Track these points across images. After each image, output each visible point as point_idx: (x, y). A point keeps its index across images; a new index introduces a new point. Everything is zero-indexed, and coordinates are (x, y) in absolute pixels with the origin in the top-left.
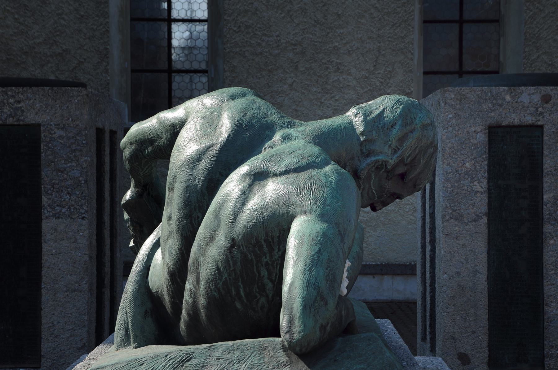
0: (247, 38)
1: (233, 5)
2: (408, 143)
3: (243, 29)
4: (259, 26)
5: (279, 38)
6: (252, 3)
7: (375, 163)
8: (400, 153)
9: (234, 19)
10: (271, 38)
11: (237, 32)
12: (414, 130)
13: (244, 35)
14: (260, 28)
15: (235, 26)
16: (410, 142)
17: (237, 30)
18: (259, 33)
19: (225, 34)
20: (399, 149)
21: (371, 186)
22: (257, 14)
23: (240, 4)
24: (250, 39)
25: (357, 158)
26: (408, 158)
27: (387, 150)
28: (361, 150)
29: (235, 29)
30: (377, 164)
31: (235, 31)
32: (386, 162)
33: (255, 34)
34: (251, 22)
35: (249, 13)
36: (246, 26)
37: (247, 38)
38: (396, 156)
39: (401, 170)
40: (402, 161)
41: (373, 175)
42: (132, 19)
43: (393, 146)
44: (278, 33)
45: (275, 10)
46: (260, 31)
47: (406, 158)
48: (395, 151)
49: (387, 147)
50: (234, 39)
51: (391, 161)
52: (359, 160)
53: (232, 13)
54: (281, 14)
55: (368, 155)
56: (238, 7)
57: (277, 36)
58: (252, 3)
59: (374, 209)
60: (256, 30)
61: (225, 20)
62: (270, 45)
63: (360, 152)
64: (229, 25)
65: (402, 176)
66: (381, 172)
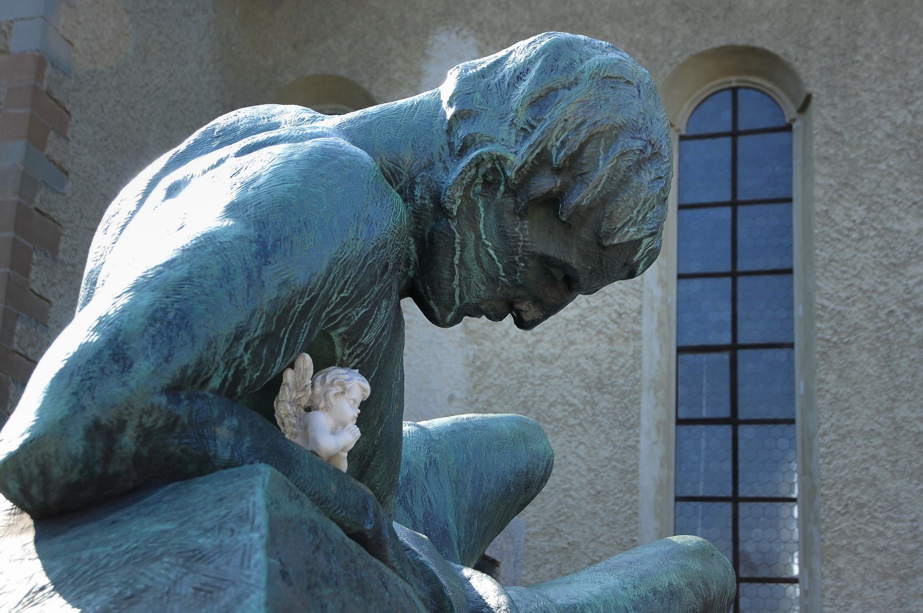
0: (861, 524)
1: (835, 471)
2: (557, 113)
3: (852, 509)
4: (879, 504)
5: (915, 524)
6: (868, 469)
7: (477, 165)
8: (536, 135)
9: (836, 494)
10: (901, 525)
11: (844, 514)
12: (576, 82)
13: (854, 519)
14: (881, 507)
15: (839, 505)
16: (565, 108)
17: (843, 511)
18: (881, 516)
19: (823, 517)
20: (533, 127)
21: (479, 237)
22: (876, 485)
23: (847, 470)
24: (866, 524)
25: (441, 165)
26: (559, 151)
27: (505, 133)
28: (450, 144)
29: (839, 509)
30: (482, 171)
31: (838, 512)
32: (501, 159)
33: (873, 517)
34: (865, 497)
35: (863, 484)
36: (858, 504)
37: (861, 524)
38: (526, 145)
39: (545, 184)
40: (542, 161)
41: (480, 204)
42: (678, 499)
43: (520, 123)
44: (913, 516)
45: (907, 479)
46: (881, 513)
47: (554, 152)
48: (525, 132)
49: (505, 127)
50: (839, 524)
51: (512, 157)
52: (446, 169)
53: (833, 484)
54: (917, 484)
55: (464, 150)
56: (843, 474)
57: (913, 521)
58: (868, 469)
59: (522, 324)
60: (875, 510)
61: (822, 495)
62: (901, 535)
63: (446, 148)
64: (829, 503)
65: (552, 201)
66: (499, 195)
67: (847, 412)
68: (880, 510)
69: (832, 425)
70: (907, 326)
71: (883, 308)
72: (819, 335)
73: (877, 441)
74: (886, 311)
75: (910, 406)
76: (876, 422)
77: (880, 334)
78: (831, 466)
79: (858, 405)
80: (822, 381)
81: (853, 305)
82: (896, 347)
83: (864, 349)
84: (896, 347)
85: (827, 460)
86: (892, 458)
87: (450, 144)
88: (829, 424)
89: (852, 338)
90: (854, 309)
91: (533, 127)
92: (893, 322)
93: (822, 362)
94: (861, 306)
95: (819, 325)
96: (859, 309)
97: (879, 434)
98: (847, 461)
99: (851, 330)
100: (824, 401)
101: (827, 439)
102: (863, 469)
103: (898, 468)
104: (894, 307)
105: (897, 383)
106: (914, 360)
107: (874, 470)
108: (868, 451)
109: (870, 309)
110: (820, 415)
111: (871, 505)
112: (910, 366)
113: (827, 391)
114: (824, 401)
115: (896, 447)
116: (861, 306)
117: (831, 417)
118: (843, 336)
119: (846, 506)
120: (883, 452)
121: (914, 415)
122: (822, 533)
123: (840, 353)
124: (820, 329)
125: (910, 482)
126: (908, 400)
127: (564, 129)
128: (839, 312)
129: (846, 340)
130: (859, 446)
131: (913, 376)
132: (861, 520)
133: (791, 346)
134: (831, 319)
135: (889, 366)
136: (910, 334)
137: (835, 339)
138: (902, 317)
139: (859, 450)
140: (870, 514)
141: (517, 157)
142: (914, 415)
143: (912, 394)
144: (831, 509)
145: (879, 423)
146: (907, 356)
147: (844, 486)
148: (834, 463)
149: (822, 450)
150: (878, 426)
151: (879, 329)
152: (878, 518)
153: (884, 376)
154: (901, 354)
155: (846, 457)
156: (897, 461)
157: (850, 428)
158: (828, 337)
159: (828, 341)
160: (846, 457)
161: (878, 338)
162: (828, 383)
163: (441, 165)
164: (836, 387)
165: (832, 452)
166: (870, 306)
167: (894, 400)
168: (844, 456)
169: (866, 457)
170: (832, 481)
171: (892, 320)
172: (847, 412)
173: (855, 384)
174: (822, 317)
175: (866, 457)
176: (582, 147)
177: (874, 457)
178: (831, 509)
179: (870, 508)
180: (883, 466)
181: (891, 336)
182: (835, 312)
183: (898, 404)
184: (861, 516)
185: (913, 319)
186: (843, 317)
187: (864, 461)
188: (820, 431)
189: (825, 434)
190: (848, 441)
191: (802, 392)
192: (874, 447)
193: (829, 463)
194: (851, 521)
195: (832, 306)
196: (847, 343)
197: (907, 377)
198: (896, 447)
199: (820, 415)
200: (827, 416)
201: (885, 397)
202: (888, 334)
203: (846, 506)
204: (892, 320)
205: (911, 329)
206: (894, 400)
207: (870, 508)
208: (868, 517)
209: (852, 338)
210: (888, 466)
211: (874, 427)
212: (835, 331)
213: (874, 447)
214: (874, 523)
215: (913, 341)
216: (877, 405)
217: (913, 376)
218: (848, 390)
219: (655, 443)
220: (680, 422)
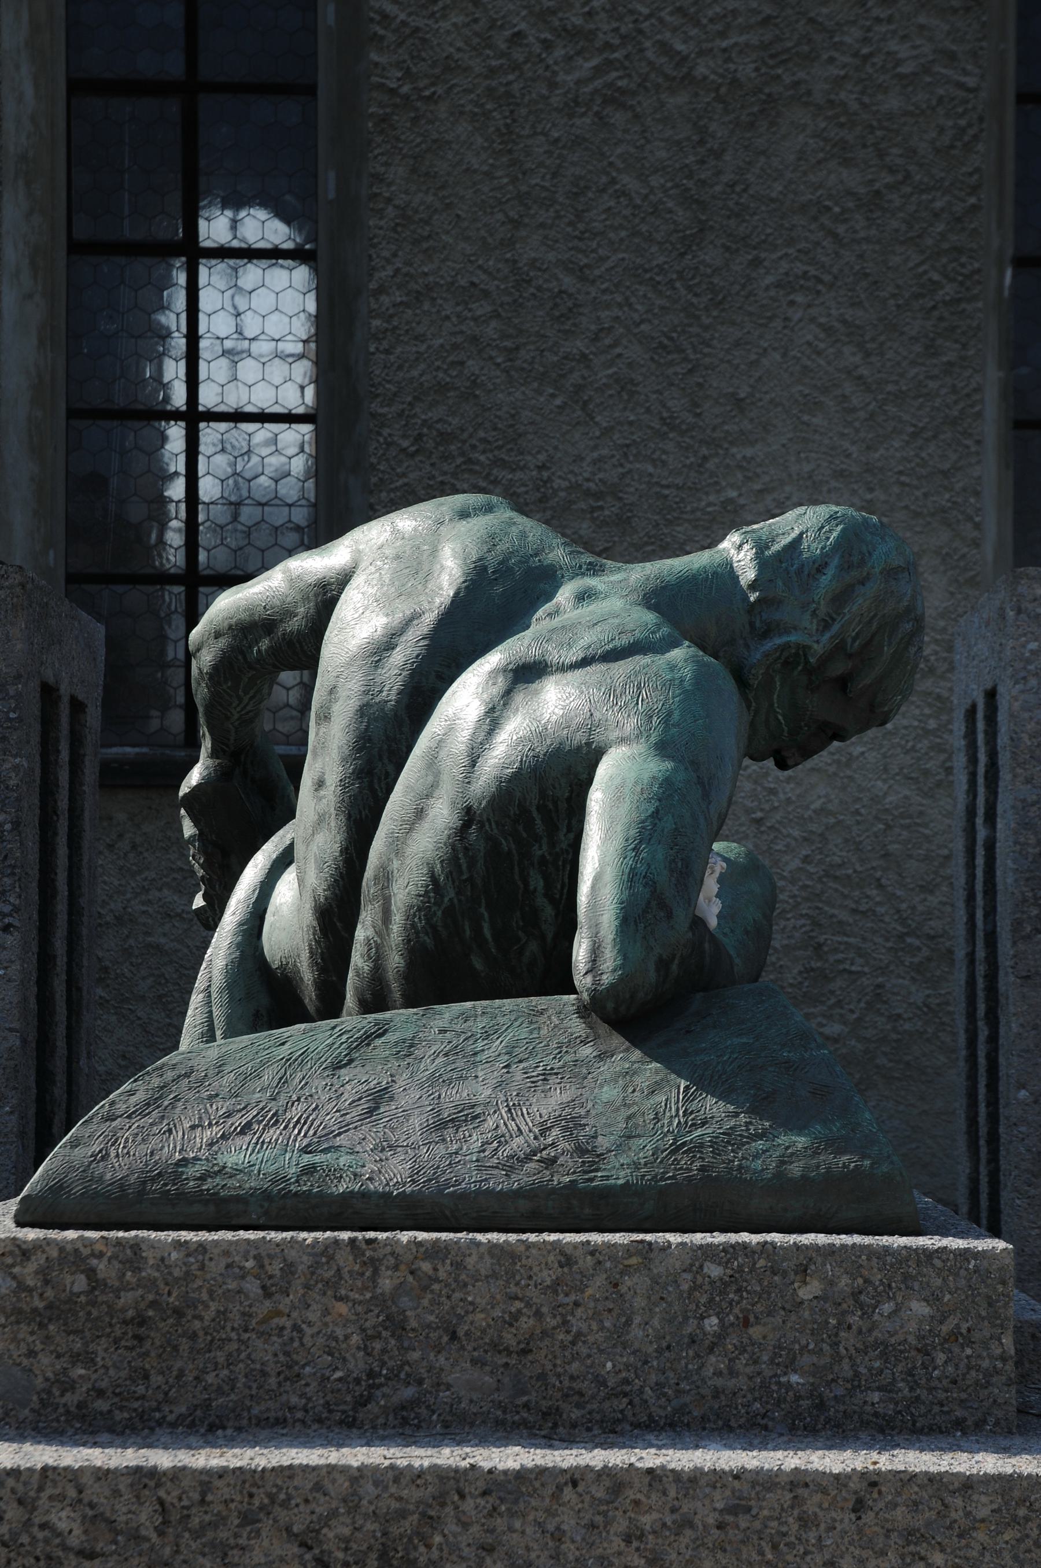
0: (445, 473)
1: (400, 368)
2: (855, 608)
3: (430, 444)
4: (481, 434)
5: (545, 474)
6: (462, 363)
7: (783, 651)
8: (836, 628)
9: (400, 414)
10: (519, 475)
11: (412, 456)
12: (868, 577)
13: (433, 465)
14: (484, 440)
15: (404, 436)
16: (860, 604)
17: (413, 449)
18: (482, 458)
19: (373, 460)
20: (834, 620)
21: (772, 705)
22: (476, 396)
23: (422, 366)
24: (454, 475)
25: (741, 642)
26: (854, 640)
27: (808, 622)
28: (752, 624)
29: (405, 444)
30: (786, 654)
31: (404, 450)
32: (806, 648)
33: (470, 461)
34: (455, 421)
35: (451, 394)
36: (441, 434)
37: (445, 473)
38: (827, 635)
39: (838, 668)
40: (839, 648)
41: (777, 679)
42: (73, 414)
44: (542, 457)
45: (535, 385)
46: (484, 452)
47: (849, 640)
48: (826, 625)
49: (807, 616)
50: (404, 475)
51: (815, 646)
52: (747, 646)
53: (395, 395)
54: (553, 396)
55: (766, 634)
56: (415, 373)
57: (542, 468)
58: (462, 363)
59: (782, 765)
60: (474, 447)
61: (373, 415)
62: (518, 496)
63: (747, 626)
64: (386, 432)
65: (843, 683)
66: (796, 673)
67: (425, 245)
68: (481, 447)
69: (397, 271)
70: (547, 67)
71: (502, 27)
72: (375, 79)
73: (482, 308)
74: (507, 33)
75: (546, 237)
76: (480, 267)
77: (494, 83)
78: (392, 358)
79: (448, 233)
80: (378, 178)
81: (444, 17)
82: (524, 111)
83: (462, 113)
84: (524, 111)
85: (385, 344)
86: (508, 344)
87: (752, 624)
88: (389, 271)
89: (440, 90)
90: (445, 25)
91: (834, 620)
92: (521, 59)
93: (379, 139)
94: (460, 19)
95: (374, 56)
96: (455, 25)
97: (486, 294)
98: (423, 348)
99: (437, 71)
100: (382, 223)
101: (385, 299)
102: (453, 363)
103: (518, 363)
104: (523, 26)
105: (524, 188)
106: (557, 140)
107: (473, 365)
108: (464, 328)
109: (476, 27)
110: (372, 251)
111: (465, 435)
112: (549, 153)
113: (389, 200)
114: (382, 223)
115: (516, 321)
116: (460, 19)
117: (395, 255)
118: (421, 85)
119: (420, 437)
120: (491, 330)
121: (551, 256)
122: (371, 492)
123: (415, 120)
124: (376, 64)
125: (539, 392)
126: (542, 225)
127: (860, 622)
128: (417, 29)
129: (427, 93)
130: (447, 318)
131: (554, 175)
132: (446, 467)
133: (311, 90)
134: (400, 45)
135: (510, 151)
136: (553, 85)
137: (405, 89)
138: (537, 48)
139: (448, 324)
140: (463, 454)
141: (820, 645)
142: (551, 256)
143: (552, 213)
144: (389, 444)
145: (485, 271)
146: (545, 134)
147: (417, 398)
148: (399, 350)
149: (376, 323)
150: (483, 277)
151: (492, 72)
152: (478, 462)
153: (499, 174)
154: (533, 127)
155: (420, 338)
156: (517, 348)
157: (431, 279)
158: (393, 85)
159: (393, 92)
160: (420, 338)
161: (490, 90)
162: (389, 185)
163: (741, 642)
164: (406, 192)
165: (395, 328)
166: (476, 21)
167: (517, 224)
168: (416, 338)
169: (459, 339)
170: (392, 388)
171: (518, 55)
172: (425, 245)
173: (443, 187)
174: (382, 38)
175: (459, 339)
176: (873, 636)
177: (474, 339)
178: (389, 444)
179: (464, 442)
180: (491, 358)
181: (516, 87)
182: (408, 31)
183: (523, 233)
184: (446, 457)
185: (559, 53)
186: (424, 40)
187: (455, 347)
188: (373, 285)
189: (381, 290)
190: (426, 306)
191: (332, 195)
192: (475, 319)
193: (387, 352)
194: (428, 468)
195: (402, 16)
196: (430, 98)
197: (543, 178)
198: (516, 321)
199: (372, 251)
200: (386, 254)
201: (500, 216)
202: (509, 83)
203: (420, 437)
204: (518, 55)
205: (555, 73)
206: (517, 224)
207: (464, 442)
208: (459, 460)
209: (440, 90)
210: (499, 360)
211: (475, 280)
212: (408, 71)
213: (475, 319)
214: (471, 471)
215: (555, 101)
216: (483, 233)
217: (554, 175)
218: (430, 199)
219: (30, 296)
220: (76, 248)
